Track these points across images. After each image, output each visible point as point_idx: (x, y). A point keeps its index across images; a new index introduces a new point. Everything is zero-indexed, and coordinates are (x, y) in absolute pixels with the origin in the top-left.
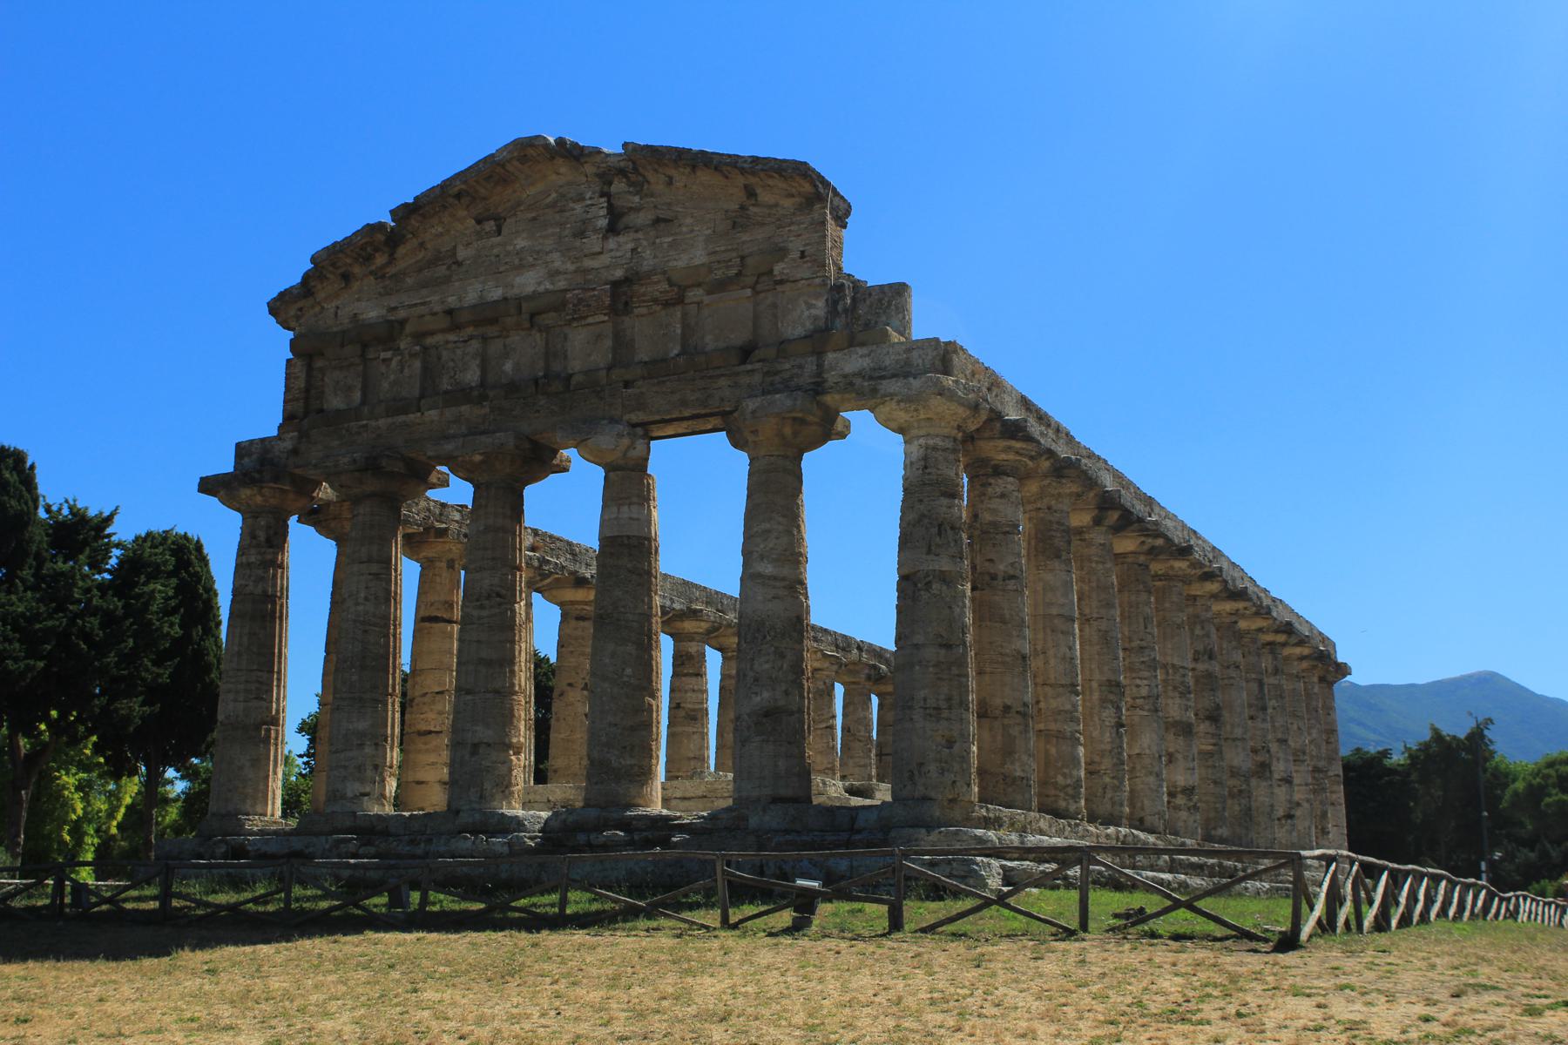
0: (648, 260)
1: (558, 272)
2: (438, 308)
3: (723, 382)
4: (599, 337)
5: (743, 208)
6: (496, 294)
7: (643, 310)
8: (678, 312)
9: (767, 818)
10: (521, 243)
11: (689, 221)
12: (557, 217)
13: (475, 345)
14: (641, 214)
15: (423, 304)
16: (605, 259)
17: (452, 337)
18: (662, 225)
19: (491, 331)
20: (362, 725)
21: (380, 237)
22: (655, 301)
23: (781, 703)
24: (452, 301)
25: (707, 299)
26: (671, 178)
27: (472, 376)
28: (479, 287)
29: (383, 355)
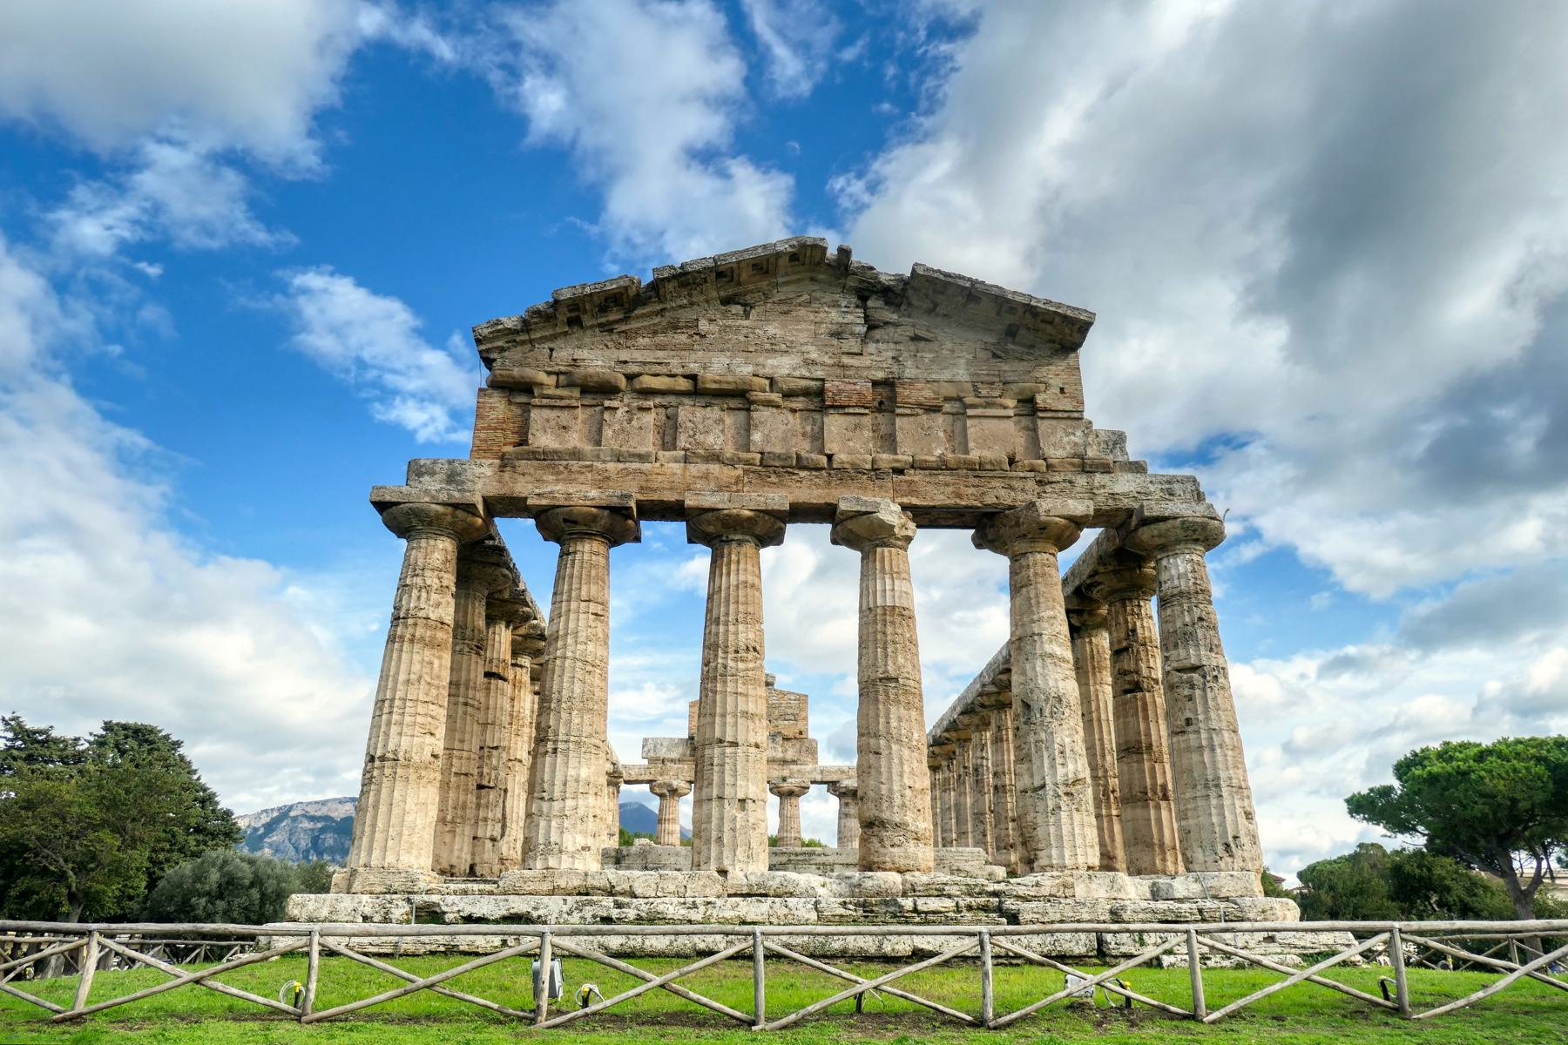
0: (910, 372)
1: (814, 363)
2: (680, 371)
3: (994, 483)
4: (857, 427)
6: (747, 370)
8: (940, 419)
9: (1094, 886)
10: (772, 329)
11: (949, 345)
12: (812, 317)
13: (714, 413)
14: (899, 330)
16: (865, 361)
17: (686, 400)
18: (922, 344)
19: (734, 403)
20: (584, 773)
21: (633, 292)
22: (920, 405)
23: (1081, 776)
24: (694, 367)
25: (970, 412)
26: (936, 305)
29: (607, 403)
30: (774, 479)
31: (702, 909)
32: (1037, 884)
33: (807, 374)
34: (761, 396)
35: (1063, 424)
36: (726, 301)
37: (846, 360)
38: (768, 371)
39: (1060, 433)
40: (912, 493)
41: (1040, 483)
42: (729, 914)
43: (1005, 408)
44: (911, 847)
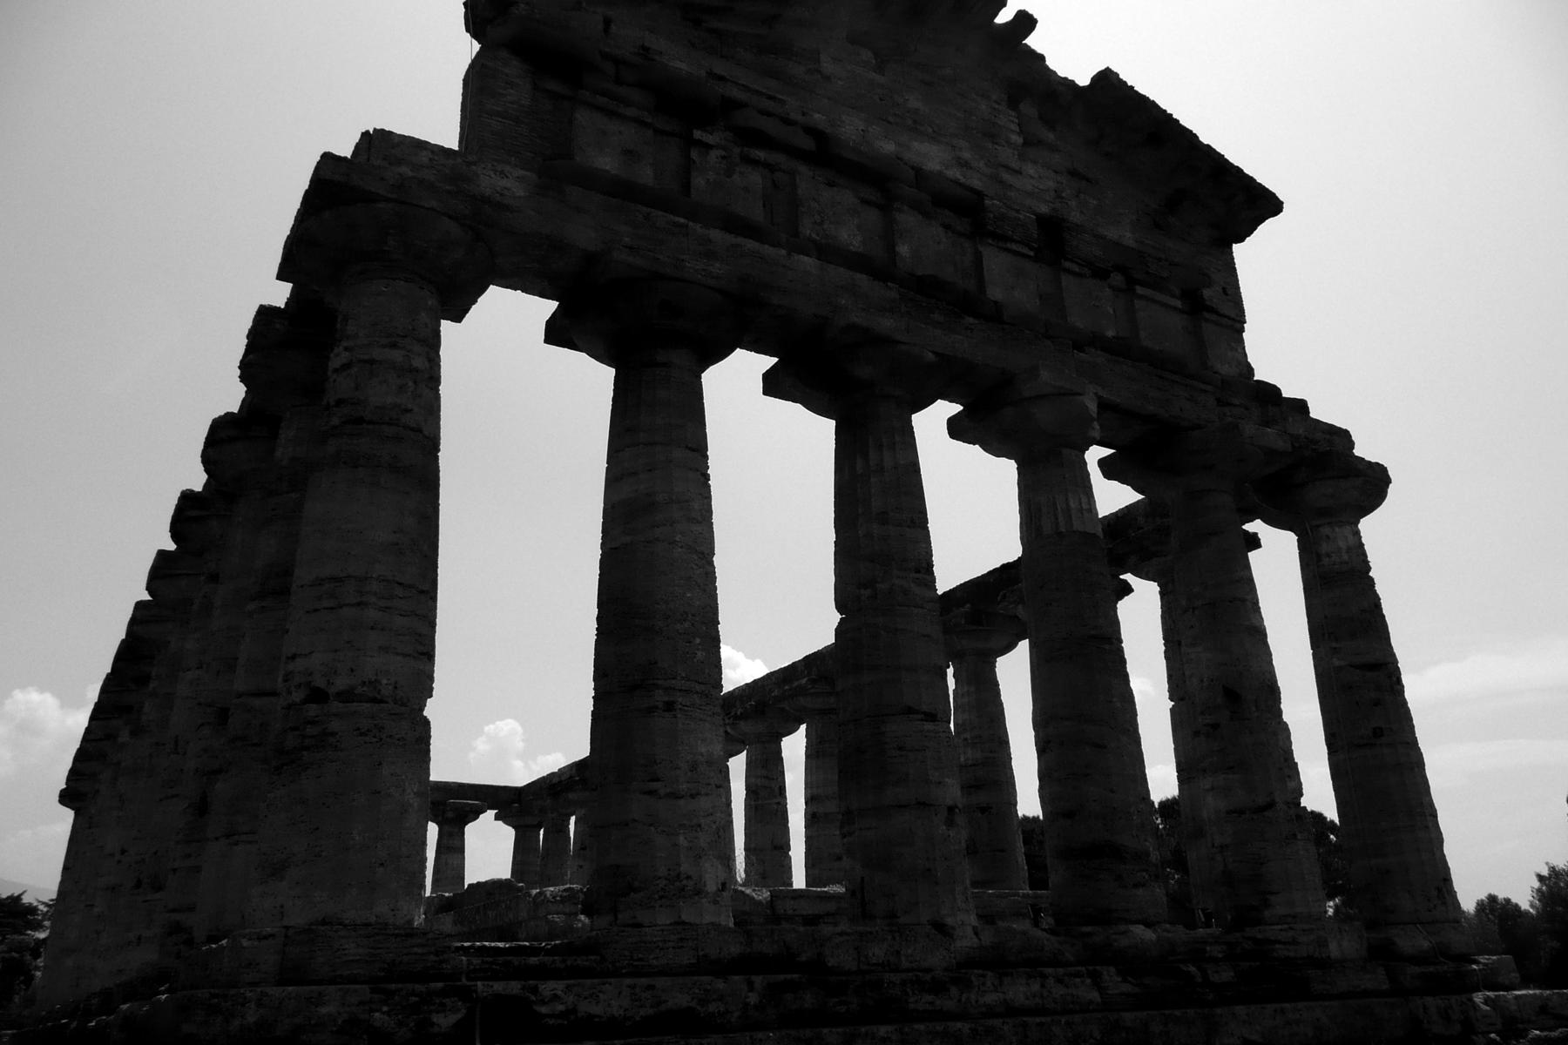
1: (964, 164)
6: (889, 147)
7: (1076, 269)
10: (914, 102)
15: (770, 98)
25: (1140, 290)
27: (849, 236)
29: (697, 134)
31: (954, 991)
32: (1294, 942)
33: (963, 180)
37: (1006, 176)
41: (1218, 400)
42: (990, 998)
43: (1173, 296)
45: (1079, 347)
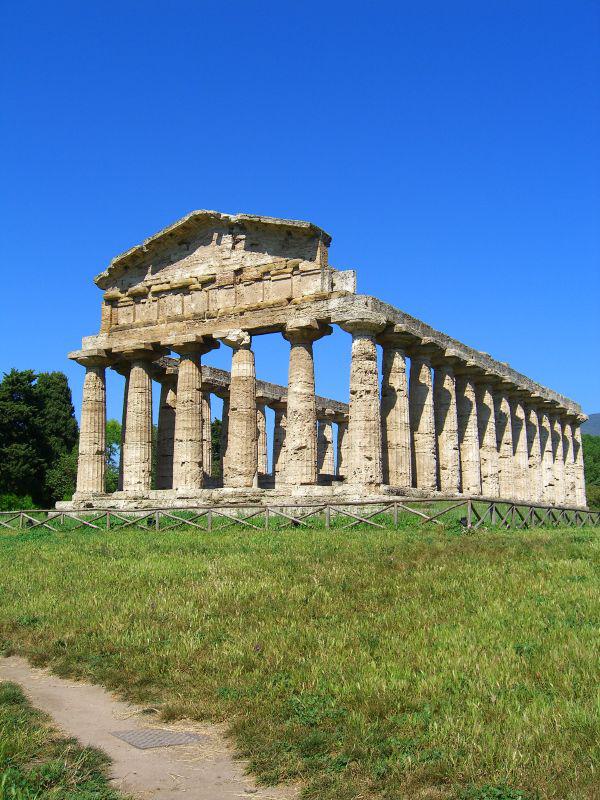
5: (286, 240)
6: (187, 275)
27: (178, 310)
28: (180, 273)
30: (197, 325)
34: (193, 287)
35: (311, 277)
36: (180, 244)
37: (225, 263)
38: (195, 275)
39: (310, 281)
40: (247, 323)
44: (238, 478)
45: (242, 314)
